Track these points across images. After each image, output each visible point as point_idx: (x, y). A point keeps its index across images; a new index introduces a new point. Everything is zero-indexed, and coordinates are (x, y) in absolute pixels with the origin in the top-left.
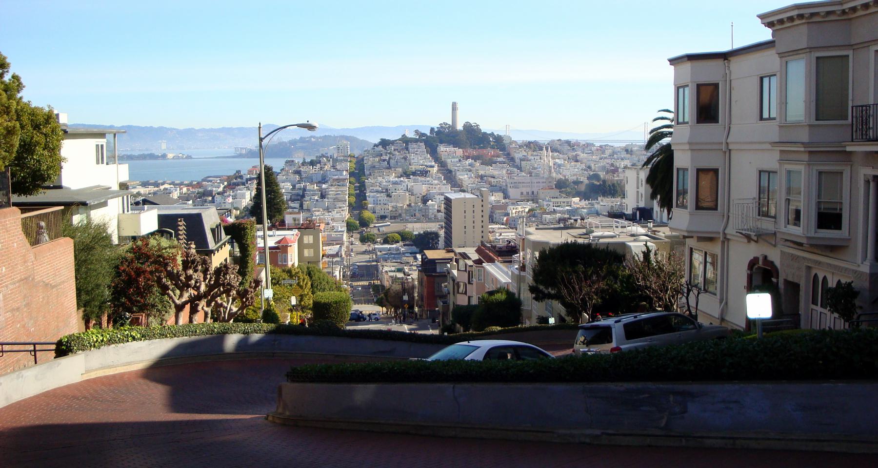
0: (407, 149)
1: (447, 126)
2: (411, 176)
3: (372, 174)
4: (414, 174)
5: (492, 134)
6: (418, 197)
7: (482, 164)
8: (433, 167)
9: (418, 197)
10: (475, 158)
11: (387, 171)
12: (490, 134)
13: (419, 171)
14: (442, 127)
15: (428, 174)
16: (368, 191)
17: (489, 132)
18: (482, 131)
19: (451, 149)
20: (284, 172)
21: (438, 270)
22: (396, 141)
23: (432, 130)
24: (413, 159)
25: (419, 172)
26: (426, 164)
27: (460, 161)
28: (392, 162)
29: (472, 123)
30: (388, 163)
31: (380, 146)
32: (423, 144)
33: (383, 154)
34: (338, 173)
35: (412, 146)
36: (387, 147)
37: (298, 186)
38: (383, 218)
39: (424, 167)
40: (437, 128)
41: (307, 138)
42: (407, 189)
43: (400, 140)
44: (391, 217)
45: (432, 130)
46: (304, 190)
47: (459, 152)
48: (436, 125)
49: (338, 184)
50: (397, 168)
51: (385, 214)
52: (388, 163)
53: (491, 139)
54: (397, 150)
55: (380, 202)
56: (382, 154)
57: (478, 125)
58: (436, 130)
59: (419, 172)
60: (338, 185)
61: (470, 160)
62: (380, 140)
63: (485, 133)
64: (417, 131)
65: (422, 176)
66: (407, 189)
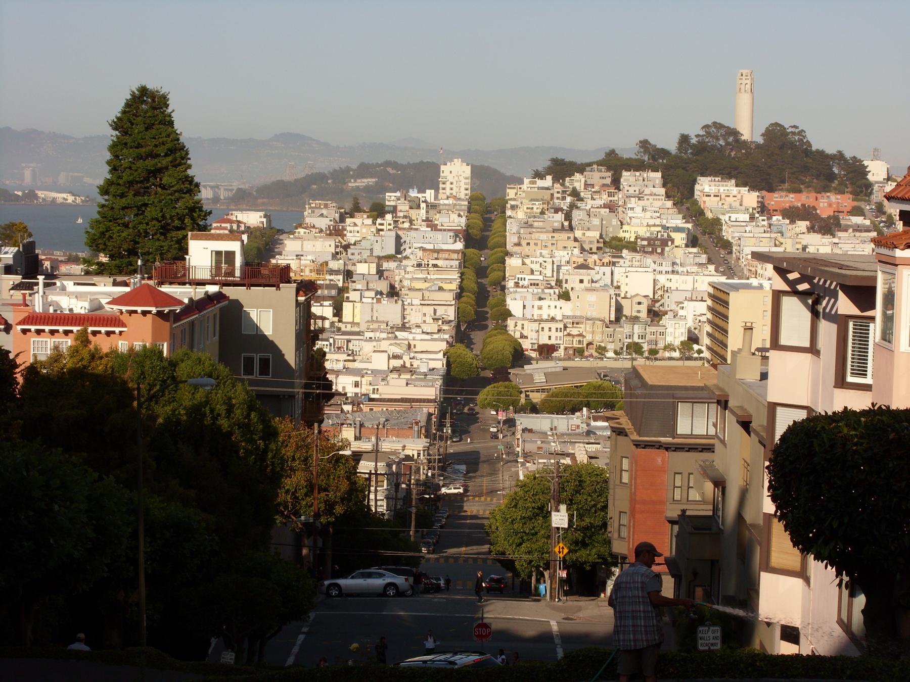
0: (616, 183)
1: (722, 131)
2: (625, 252)
3: (524, 243)
4: (632, 247)
5: (840, 156)
6: (639, 303)
7: (811, 229)
8: (677, 229)
9: (639, 303)
10: (792, 215)
11: (564, 235)
12: (832, 157)
13: (643, 239)
14: (708, 134)
15: (667, 249)
16: (510, 284)
17: (831, 150)
18: (814, 149)
19: (729, 187)
20: (302, 231)
21: (680, 431)
22: (590, 164)
23: (684, 139)
24: (632, 209)
25: (645, 243)
26: (664, 222)
27: (752, 218)
28: (576, 214)
29: (786, 126)
30: (568, 217)
31: (549, 178)
32: (658, 175)
33: (556, 195)
34: (439, 235)
35: (627, 177)
36: (567, 179)
37: (334, 265)
38: (546, 351)
39: (659, 229)
40: (697, 136)
41: (378, 165)
42: (612, 281)
43: (600, 163)
44: (566, 349)
45: (684, 139)
46: (348, 275)
47: (751, 198)
48: (694, 131)
49: (435, 262)
50: (589, 229)
51: (550, 343)
52: (568, 217)
53: (836, 170)
54: (593, 186)
55: (540, 312)
56: (552, 195)
57: (803, 131)
58: (694, 141)
59: (645, 243)
60: (435, 266)
61: (780, 218)
62: (549, 163)
63: (821, 153)
64: (644, 144)
65: (651, 253)
66: (612, 281)
